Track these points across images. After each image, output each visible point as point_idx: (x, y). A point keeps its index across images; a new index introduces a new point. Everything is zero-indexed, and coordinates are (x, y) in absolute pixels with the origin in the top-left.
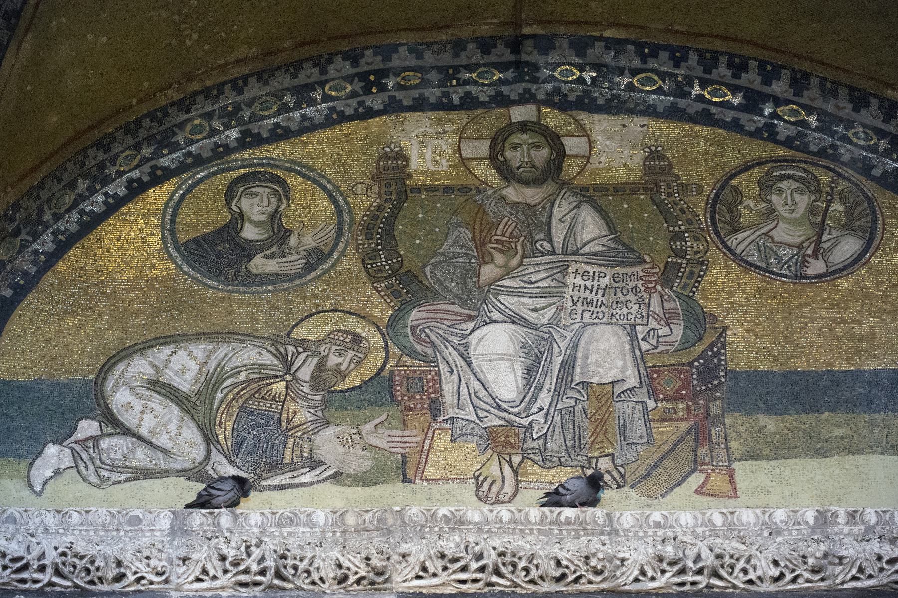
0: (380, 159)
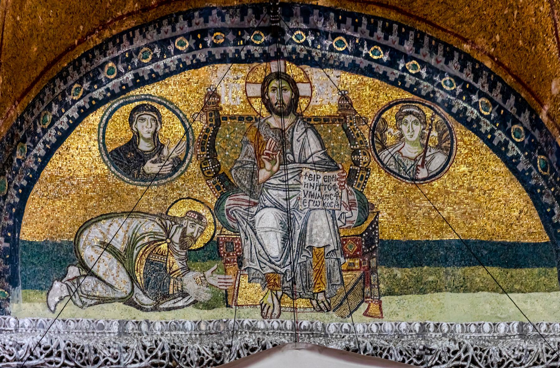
0: (206, 96)
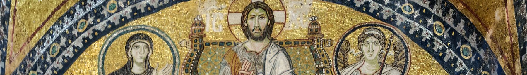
0: (193, 25)
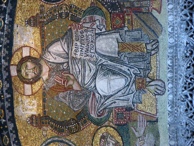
0: (32, 125)
